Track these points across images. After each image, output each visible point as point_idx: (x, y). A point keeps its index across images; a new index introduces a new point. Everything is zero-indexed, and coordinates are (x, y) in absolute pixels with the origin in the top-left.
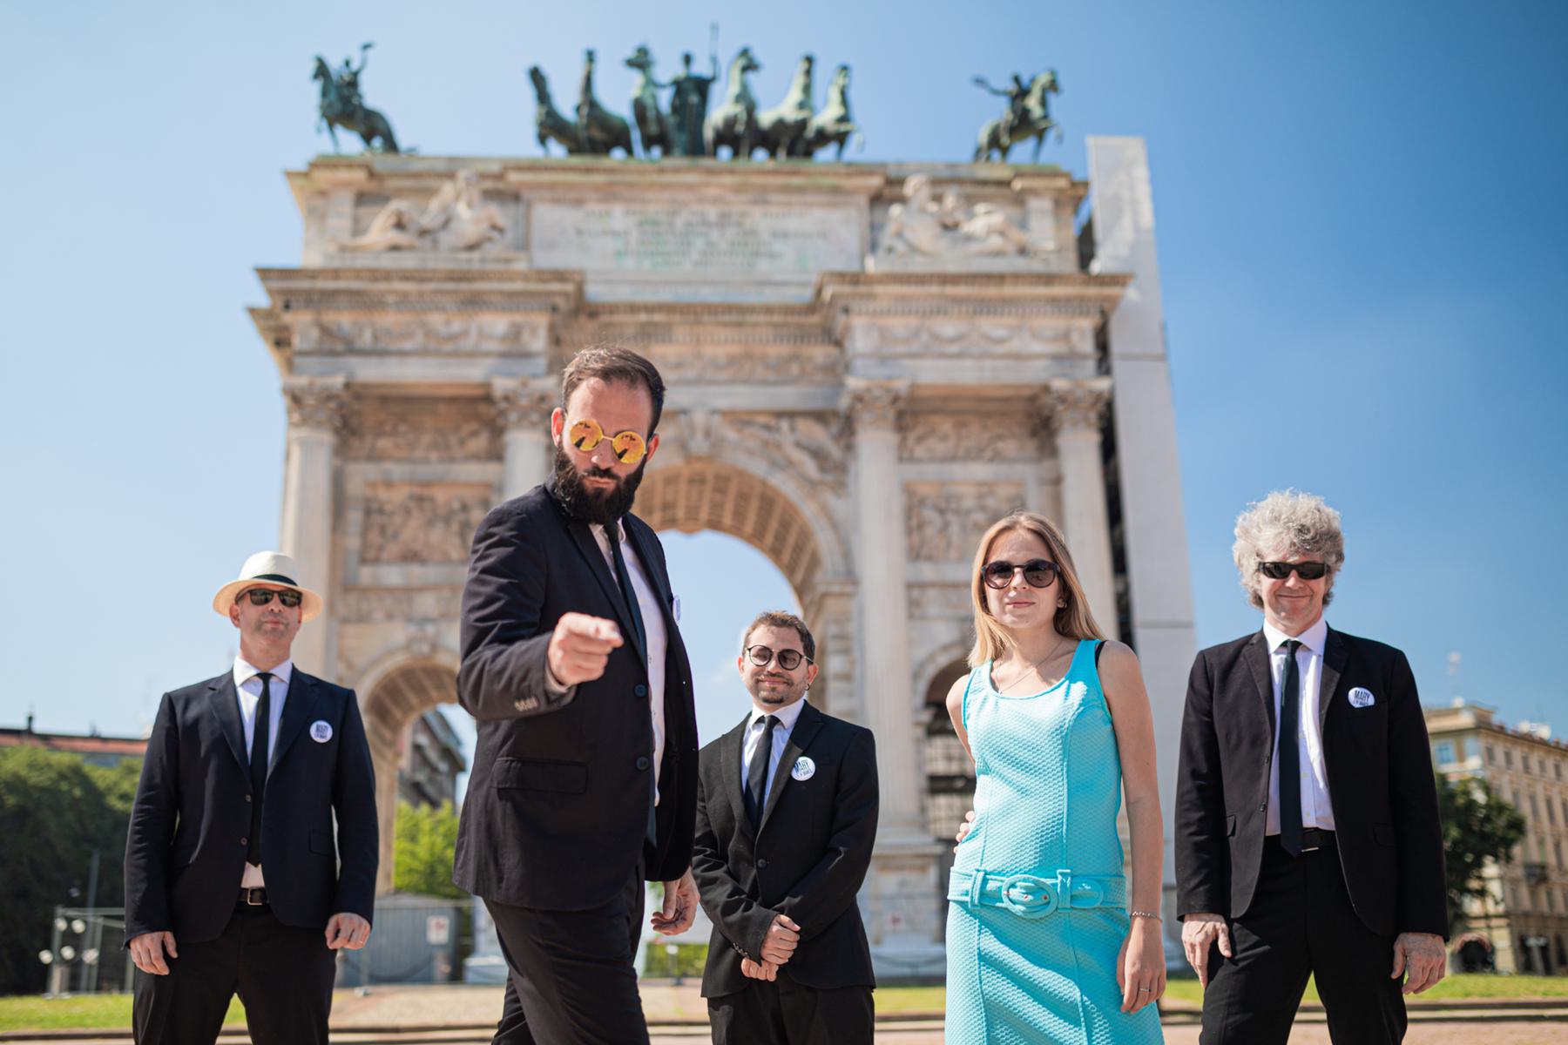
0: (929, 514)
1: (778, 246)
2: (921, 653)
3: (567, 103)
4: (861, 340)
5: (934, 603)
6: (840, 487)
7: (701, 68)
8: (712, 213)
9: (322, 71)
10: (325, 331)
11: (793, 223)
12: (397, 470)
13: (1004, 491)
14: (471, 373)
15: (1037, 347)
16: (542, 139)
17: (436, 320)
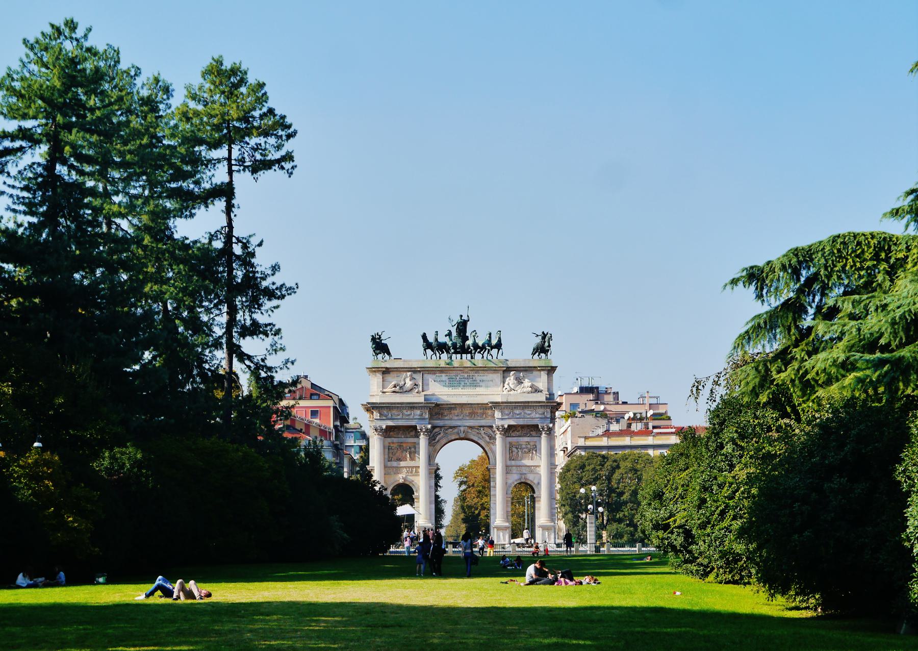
0: (514, 449)
1: (481, 384)
2: (510, 481)
3: (431, 339)
4: (498, 414)
5: (514, 470)
6: (494, 444)
7: (465, 318)
8: (466, 375)
9: (373, 339)
10: (381, 415)
11: (484, 378)
12: (395, 440)
13: (532, 444)
14: (413, 423)
15: (537, 416)
16: (425, 354)
17: (405, 411)
